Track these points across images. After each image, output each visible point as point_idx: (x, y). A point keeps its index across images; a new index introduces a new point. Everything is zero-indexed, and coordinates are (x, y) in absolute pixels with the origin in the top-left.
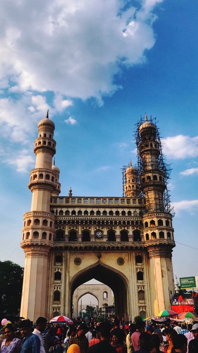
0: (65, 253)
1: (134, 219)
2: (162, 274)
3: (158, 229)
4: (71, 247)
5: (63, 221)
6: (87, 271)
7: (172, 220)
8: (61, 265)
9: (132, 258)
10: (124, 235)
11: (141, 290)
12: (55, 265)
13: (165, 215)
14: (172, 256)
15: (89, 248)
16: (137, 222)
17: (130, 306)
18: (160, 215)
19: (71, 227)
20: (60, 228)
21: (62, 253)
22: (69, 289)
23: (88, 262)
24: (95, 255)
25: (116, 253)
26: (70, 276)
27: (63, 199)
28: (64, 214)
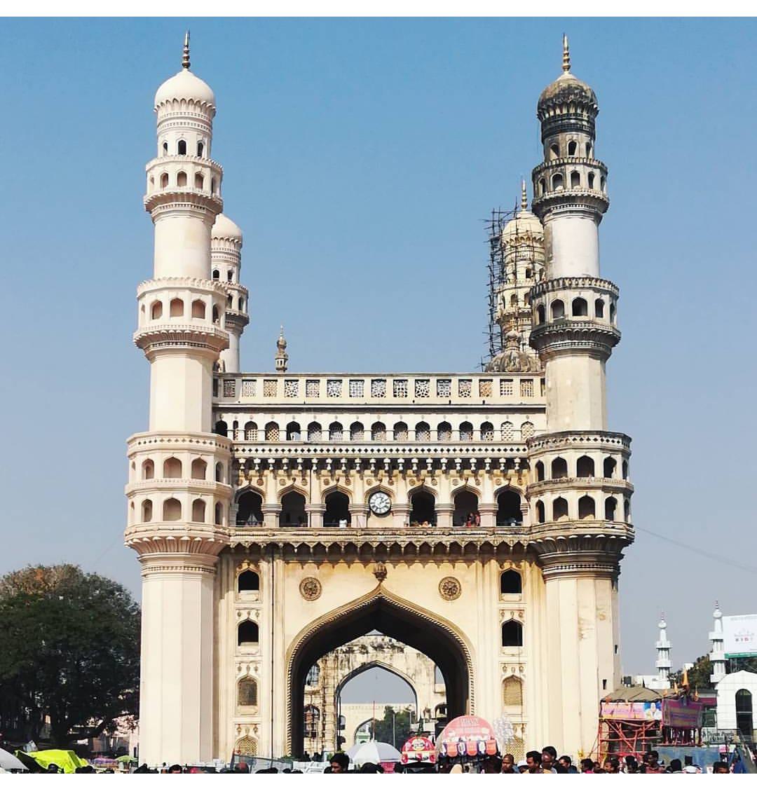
1: (499, 450)
2: (580, 629)
3: (573, 488)
4: (288, 546)
5: (257, 461)
6: (342, 617)
7: (626, 455)
8: (257, 600)
9: (487, 578)
10: (466, 503)
11: (513, 676)
12: (237, 598)
13: (602, 440)
14: (620, 573)
15: (345, 547)
16: (510, 463)
18: (585, 442)
20: (250, 483)
23: (346, 588)
28: (261, 437)
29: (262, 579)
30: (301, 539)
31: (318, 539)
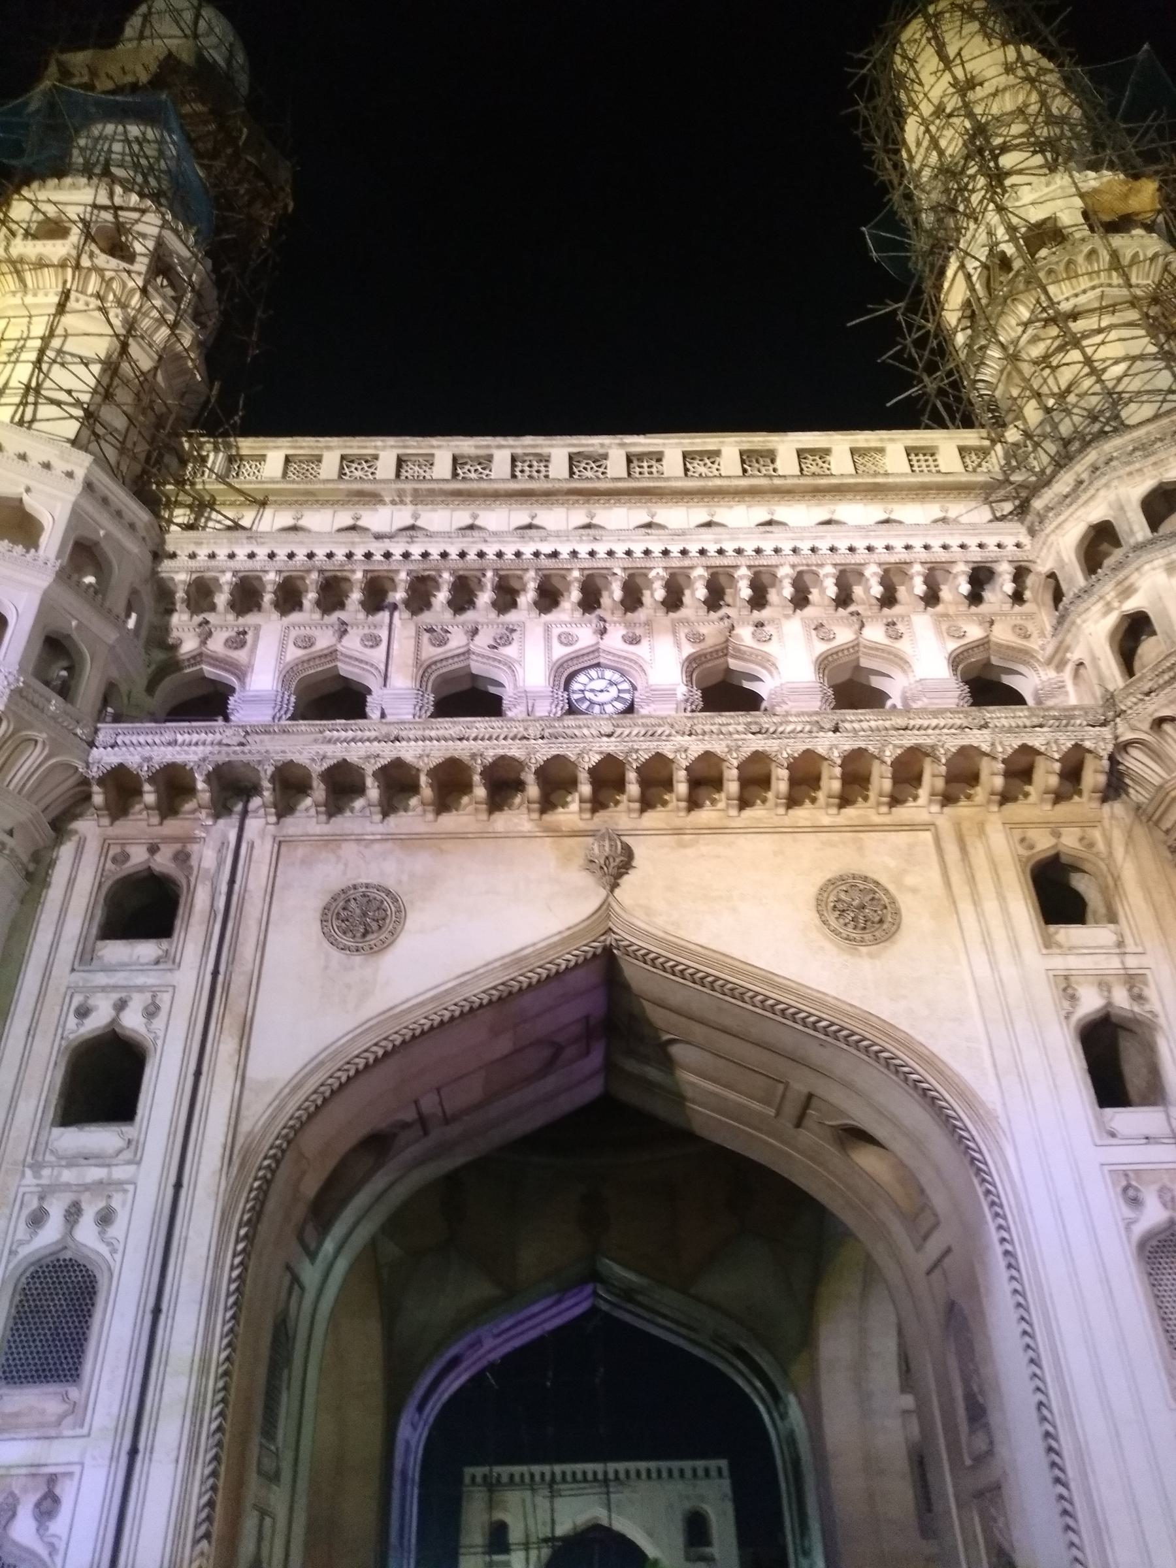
0: (224, 844)
5: (227, 578)
6: (471, 1012)
8: (157, 962)
12: (85, 958)
16: (981, 577)
17: (1066, 1444)
19: (316, 633)
20: (203, 643)
21: (193, 839)
22: (224, 1220)
24: (565, 859)
25: (796, 830)
26: (255, 1071)
27: (264, 456)
29: (192, 893)
30: (336, 753)
31: (388, 752)
